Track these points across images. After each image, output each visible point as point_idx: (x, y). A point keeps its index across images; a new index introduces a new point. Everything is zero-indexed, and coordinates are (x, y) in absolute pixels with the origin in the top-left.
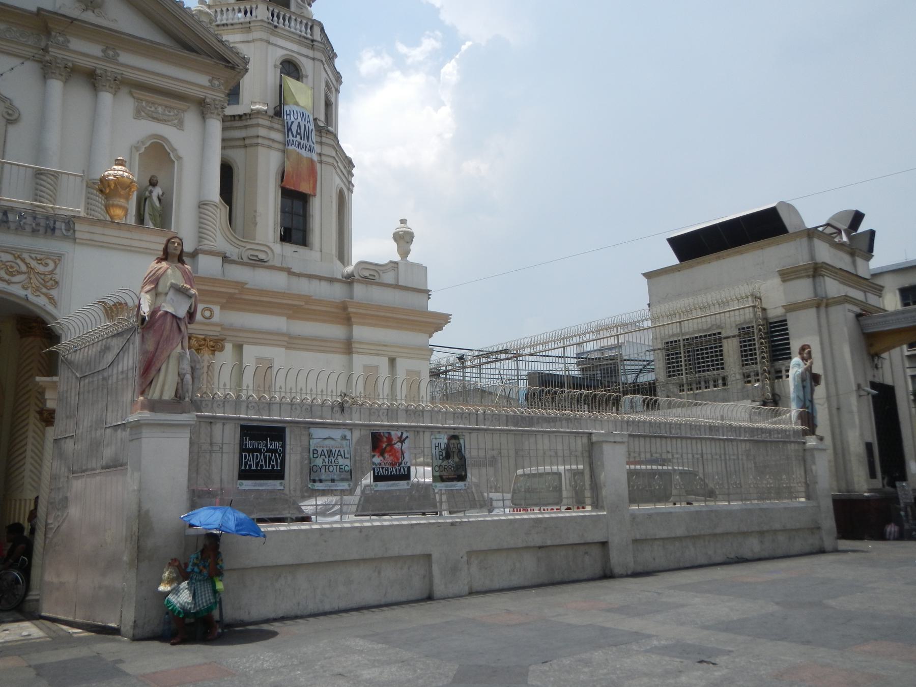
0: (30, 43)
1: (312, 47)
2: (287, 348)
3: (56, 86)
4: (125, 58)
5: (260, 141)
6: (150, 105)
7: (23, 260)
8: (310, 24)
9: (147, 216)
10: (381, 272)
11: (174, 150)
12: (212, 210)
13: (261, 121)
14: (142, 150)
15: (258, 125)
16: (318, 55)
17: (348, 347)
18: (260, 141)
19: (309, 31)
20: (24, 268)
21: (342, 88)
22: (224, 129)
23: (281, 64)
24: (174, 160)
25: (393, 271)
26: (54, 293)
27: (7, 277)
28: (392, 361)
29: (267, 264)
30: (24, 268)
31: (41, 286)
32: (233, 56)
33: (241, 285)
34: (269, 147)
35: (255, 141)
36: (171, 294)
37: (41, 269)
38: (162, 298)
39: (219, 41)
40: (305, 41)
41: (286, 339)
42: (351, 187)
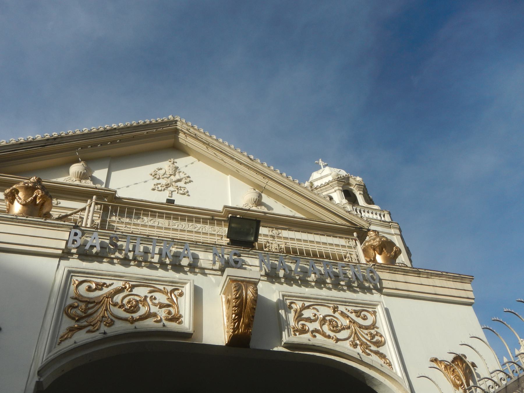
7: (342, 314)
20: (346, 322)
27: (332, 334)
30: (346, 322)
31: (368, 343)
32: (359, 220)
39: (347, 212)
40: (384, 223)
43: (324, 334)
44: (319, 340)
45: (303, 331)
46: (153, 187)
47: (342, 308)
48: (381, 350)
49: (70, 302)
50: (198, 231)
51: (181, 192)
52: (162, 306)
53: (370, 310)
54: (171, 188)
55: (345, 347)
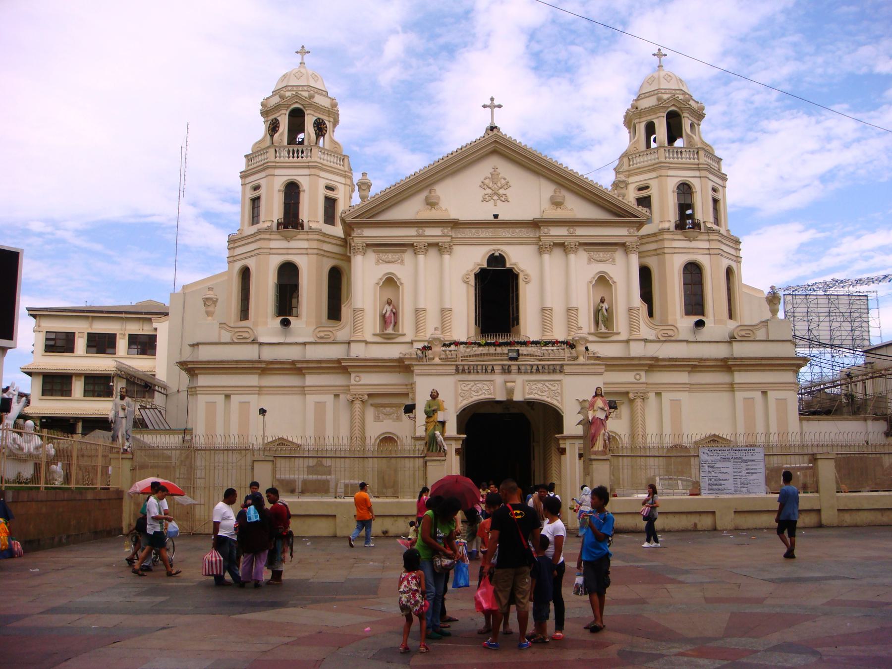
0: (531, 236)
1: (699, 169)
2: (689, 391)
3: (546, 257)
4: (580, 231)
5: (666, 250)
6: (596, 253)
7: (546, 385)
8: (696, 151)
9: (600, 322)
10: (754, 331)
11: (611, 278)
12: (635, 312)
13: (666, 236)
14: (594, 282)
15: (663, 240)
16: (704, 173)
17: (732, 387)
18: (666, 250)
19: (696, 156)
20: (547, 389)
21: (728, 184)
22: (640, 257)
23: (678, 188)
24: (612, 284)
25: (764, 328)
26: (559, 398)
27: (541, 394)
28: (764, 393)
29: (673, 339)
30: (547, 389)
33: (656, 359)
34: (673, 253)
35: (662, 251)
36: (599, 410)
37: (553, 388)
38: (596, 412)
41: (688, 386)
42: (739, 259)
43: (538, 394)
44: (537, 397)
45: (531, 393)
46: (482, 199)
47: (546, 384)
48: (557, 398)
49: (461, 391)
50: (516, 236)
51: (503, 199)
52: (486, 390)
53: (557, 383)
54: (495, 197)
55: (545, 398)
